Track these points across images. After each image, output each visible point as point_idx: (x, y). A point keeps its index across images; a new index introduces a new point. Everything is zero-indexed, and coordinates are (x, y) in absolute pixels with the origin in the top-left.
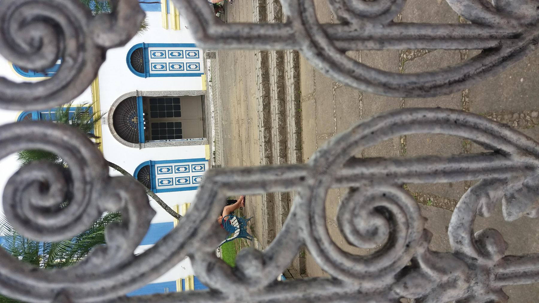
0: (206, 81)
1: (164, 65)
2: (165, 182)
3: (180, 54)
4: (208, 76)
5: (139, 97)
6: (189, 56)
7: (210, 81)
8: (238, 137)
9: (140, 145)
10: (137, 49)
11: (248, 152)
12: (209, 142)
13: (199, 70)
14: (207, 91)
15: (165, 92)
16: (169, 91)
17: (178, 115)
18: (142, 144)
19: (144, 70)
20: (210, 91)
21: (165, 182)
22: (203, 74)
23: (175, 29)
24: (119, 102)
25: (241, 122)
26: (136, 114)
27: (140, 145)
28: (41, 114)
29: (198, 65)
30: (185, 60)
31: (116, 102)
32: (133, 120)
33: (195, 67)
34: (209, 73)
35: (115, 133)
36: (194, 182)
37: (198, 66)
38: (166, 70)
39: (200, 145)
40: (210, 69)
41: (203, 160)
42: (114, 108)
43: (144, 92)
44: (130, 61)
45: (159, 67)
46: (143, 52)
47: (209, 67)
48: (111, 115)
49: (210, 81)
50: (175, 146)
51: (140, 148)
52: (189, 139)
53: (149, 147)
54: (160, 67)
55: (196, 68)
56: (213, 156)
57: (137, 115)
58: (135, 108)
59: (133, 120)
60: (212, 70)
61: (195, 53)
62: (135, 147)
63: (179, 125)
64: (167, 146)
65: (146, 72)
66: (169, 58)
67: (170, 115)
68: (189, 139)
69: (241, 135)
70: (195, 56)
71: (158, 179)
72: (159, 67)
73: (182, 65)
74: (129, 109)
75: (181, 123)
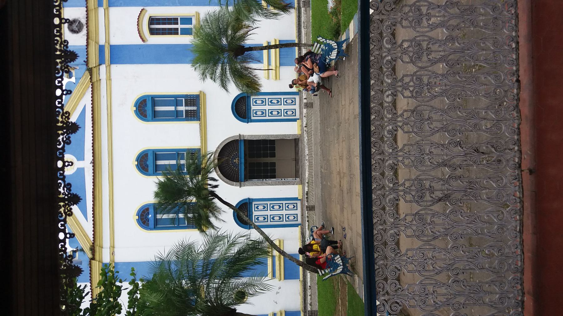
0: (302, 126)
1: (264, 111)
2: (261, 219)
3: (278, 102)
4: (304, 122)
5: (241, 140)
6: (287, 103)
7: (305, 127)
8: (339, 186)
9: (240, 184)
10: (241, 98)
11: (350, 201)
12: (302, 182)
13: (295, 116)
14: (302, 135)
15: (264, 135)
16: (268, 135)
17: (273, 155)
18: (242, 183)
19: (246, 116)
20: (305, 135)
21: (261, 219)
22: (298, 119)
23: (275, 79)
24: (224, 144)
25: (342, 175)
26: (237, 156)
27: (240, 184)
28: (155, 154)
29: (294, 111)
30: (282, 107)
31: (221, 144)
32: (235, 161)
33: (291, 113)
34: (305, 119)
35: (219, 173)
36: (287, 220)
37: (294, 112)
38: (266, 116)
39: (293, 185)
40: (306, 115)
41: (296, 199)
43: (246, 136)
44: (234, 108)
45: (259, 113)
46: (246, 100)
47: (305, 114)
48: (216, 156)
49: (305, 127)
50: (271, 185)
51: (240, 187)
52: (283, 179)
53: (248, 185)
54: (261, 113)
55: (292, 114)
56: (306, 196)
57: (238, 157)
58: (237, 150)
59: (235, 161)
60: (307, 117)
61: (292, 100)
62: (236, 185)
63: (273, 164)
64: (264, 185)
65: (248, 118)
66: (269, 105)
67: (266, 156)
68: (283, 179)
69: (342, 186)
70: (292, 103)
71: (255, 216)
72: (259, 113)
73: (280, 111)
74: (232, 151)
75: (275, 163)
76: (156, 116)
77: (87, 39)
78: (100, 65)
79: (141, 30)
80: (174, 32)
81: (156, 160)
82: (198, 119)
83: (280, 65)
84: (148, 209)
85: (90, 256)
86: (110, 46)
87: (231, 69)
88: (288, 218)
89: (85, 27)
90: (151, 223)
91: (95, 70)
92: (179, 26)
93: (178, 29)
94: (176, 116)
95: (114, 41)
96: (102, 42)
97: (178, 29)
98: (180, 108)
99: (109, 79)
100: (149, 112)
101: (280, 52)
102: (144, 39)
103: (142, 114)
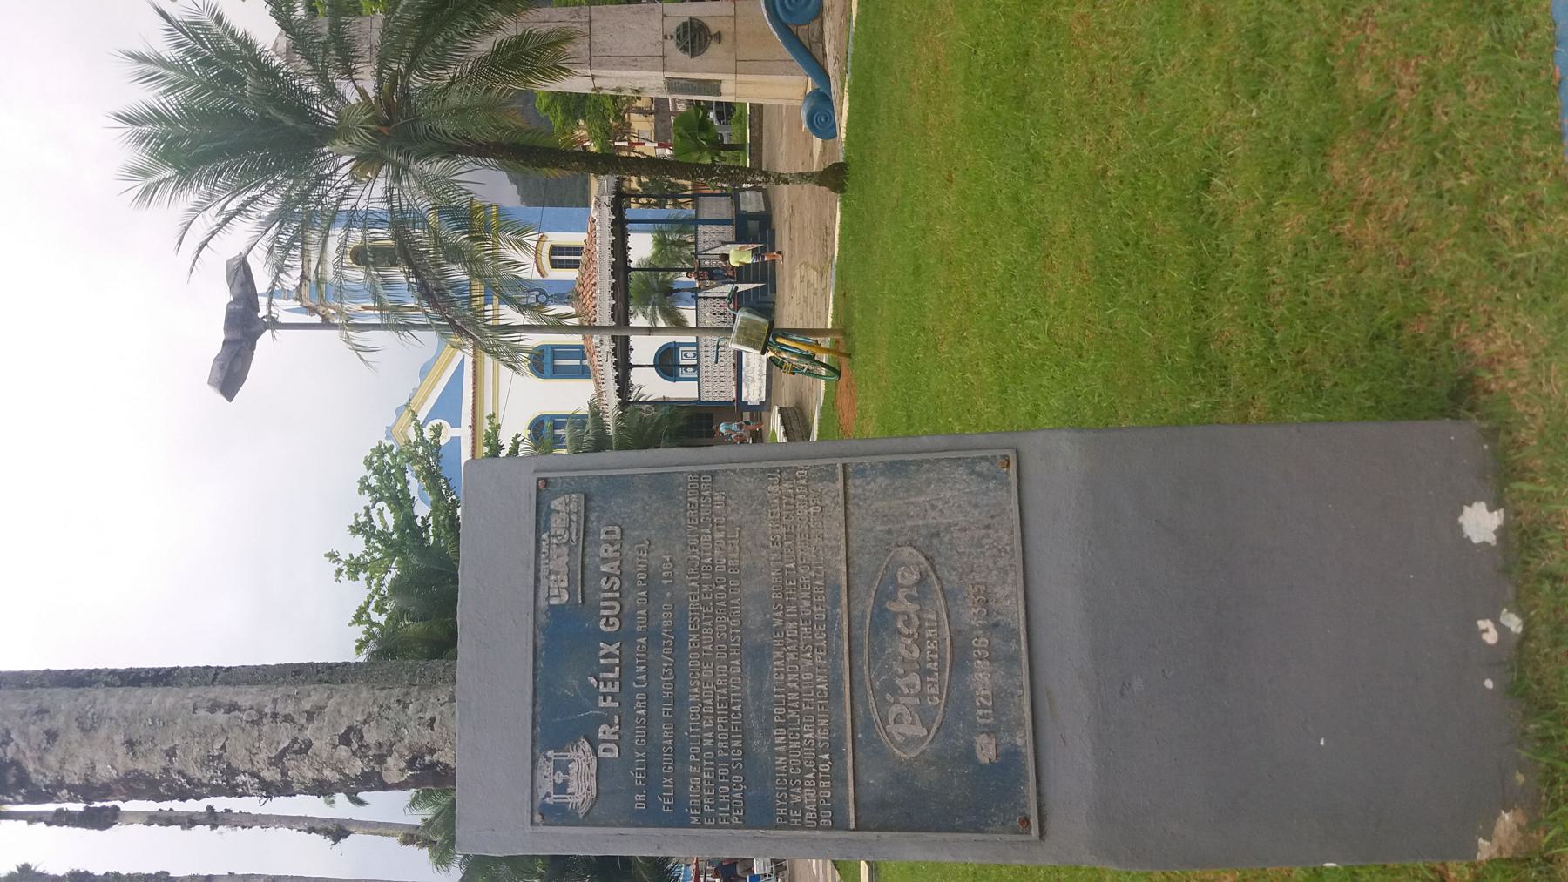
76: (557, 373)
81: (554, 429)
87: (660, 309)
100: (547, 368)
103: (537, 369)
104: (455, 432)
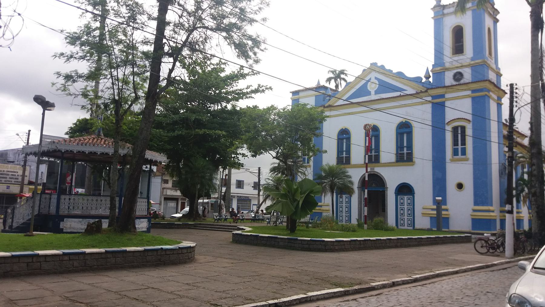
24: (383, 179)
27: (360, 188)
29: (403, 225)
42: (379, 175)
77: (448, 86)
78: (431, 96)
79: (456, 121)
80: (455, 143)
81: (375, 136)
82: (397, 161)
83: (431, 217)
84: (348, 134)
85: (326, 105)
86: (444, 102)
88: (341, 216)
89: (457, 83)
90: (341, 137)
91: (427, 94)
92: (460, 147)
93: (458, 146)
94: (399, 146)
95: (447, 104)
96: (447, 96)
97: (458, 146)
98: (405, 149)
99: (422, 103)
100: (402, 130)
101: (435, 217)
102: (449, 124)
104: (373, 92)
